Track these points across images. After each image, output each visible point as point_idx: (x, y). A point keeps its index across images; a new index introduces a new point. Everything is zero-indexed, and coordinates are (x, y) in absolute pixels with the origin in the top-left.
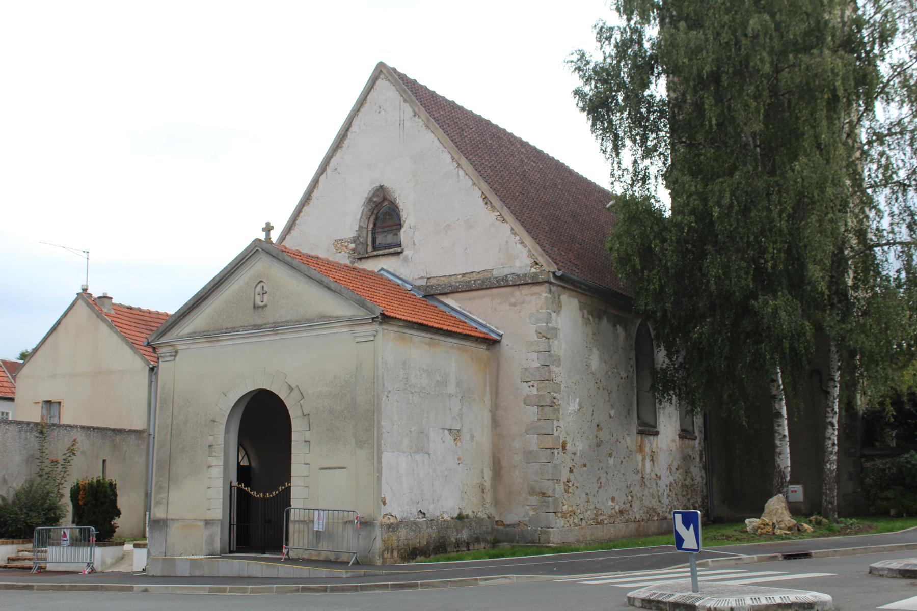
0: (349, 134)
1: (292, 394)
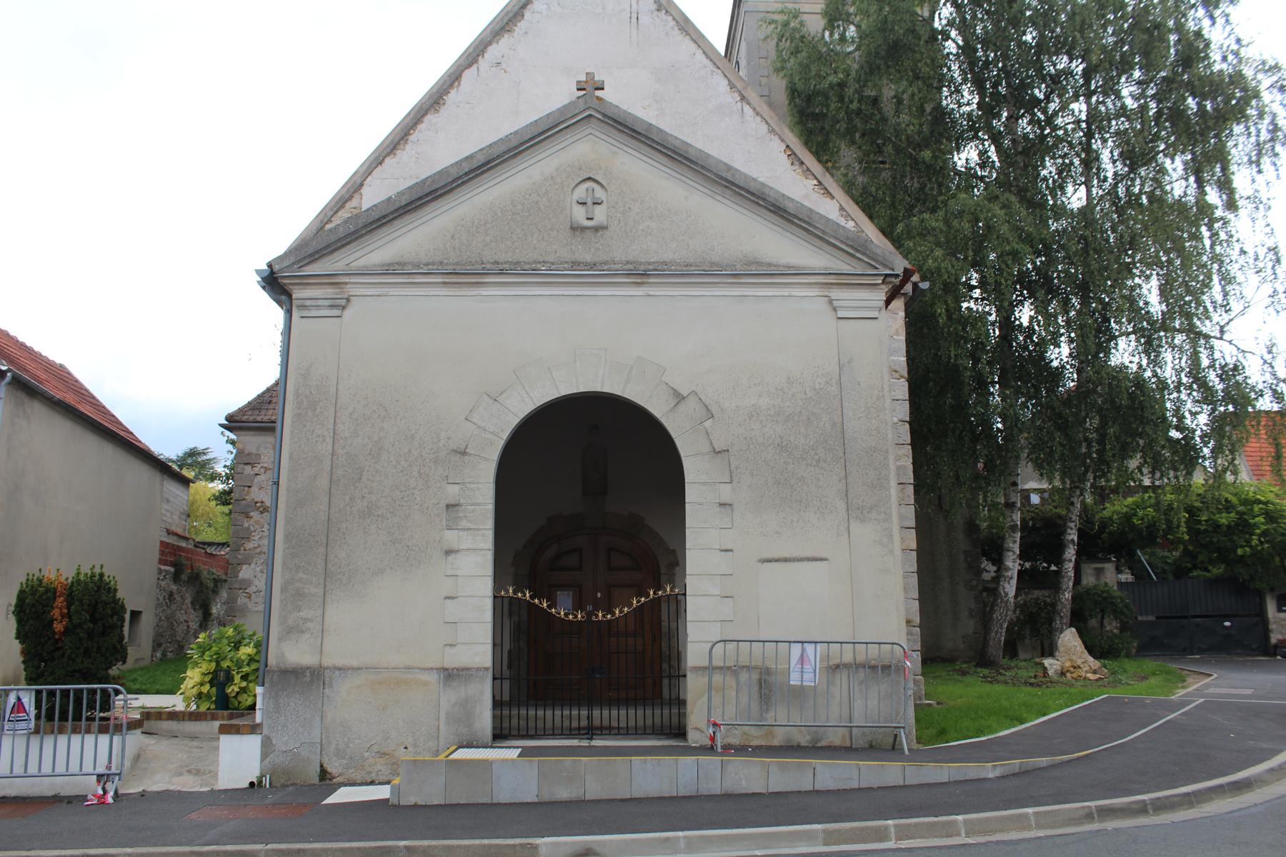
0: (527, 14)
1: (682, 407)
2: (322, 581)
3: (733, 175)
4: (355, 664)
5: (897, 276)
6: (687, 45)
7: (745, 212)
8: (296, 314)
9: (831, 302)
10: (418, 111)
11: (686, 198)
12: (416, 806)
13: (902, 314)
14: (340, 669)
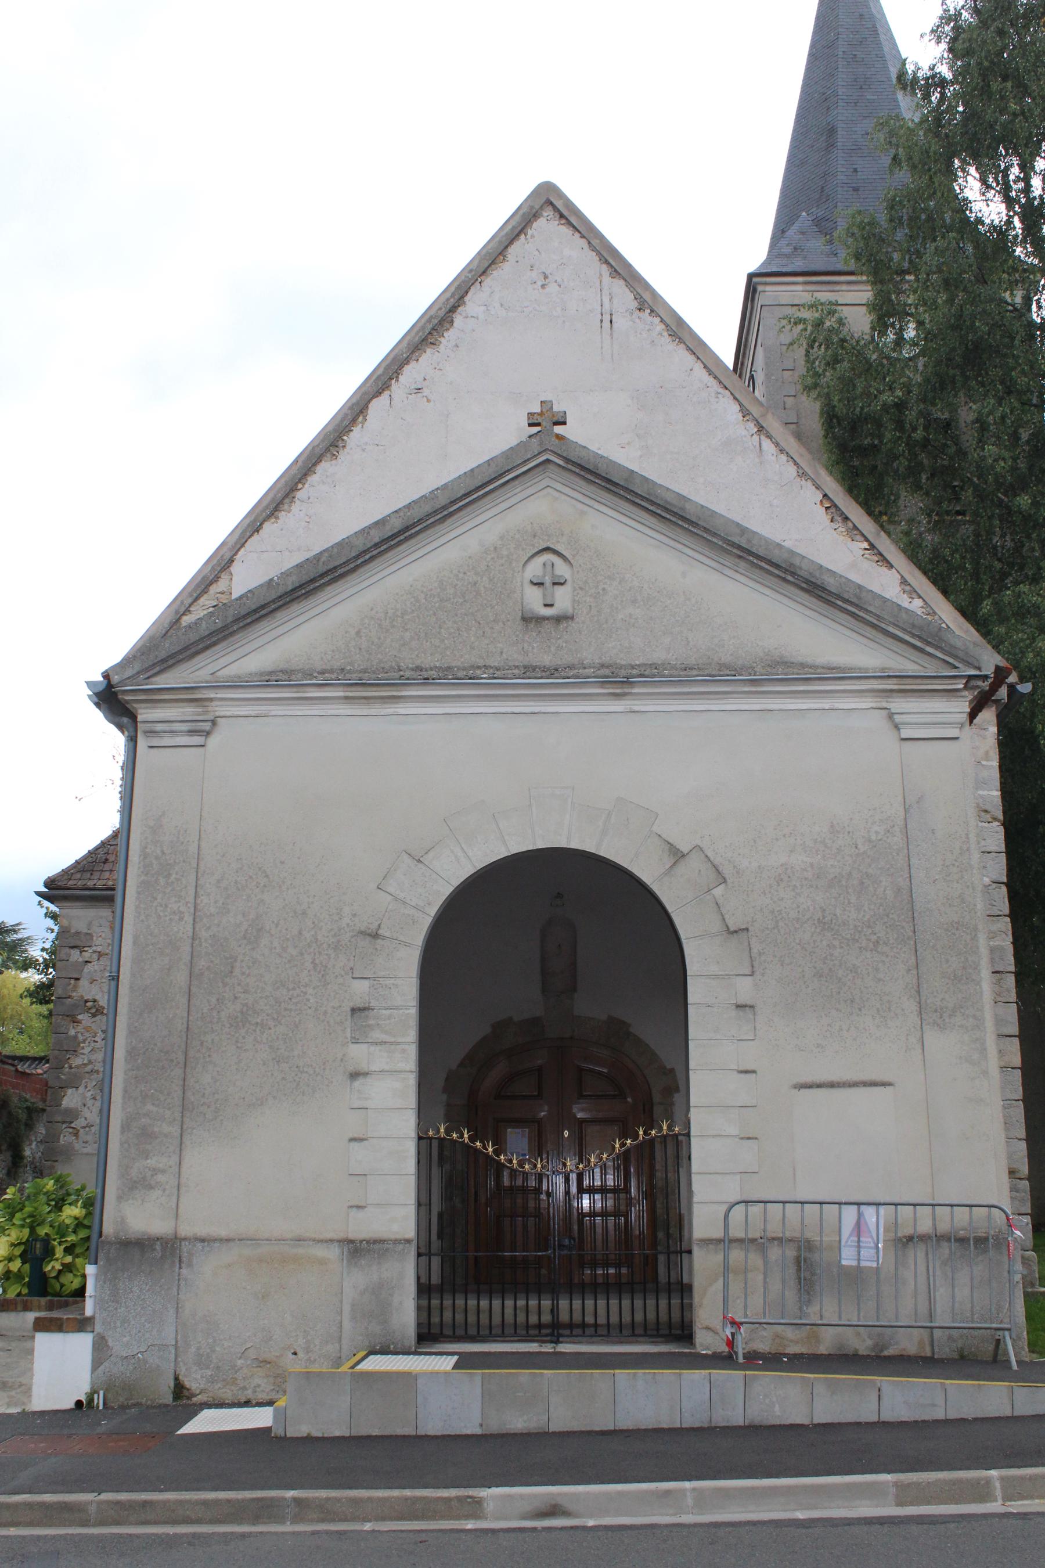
0: (458, 320)
2: (178, 1115)
3: (749, 541)
4: (223, 1233)
5: (985, 677)
6: (681, 355)
7: (768, 591)
8: (142, 742)
9: (891, 716)
10: (309, 458)
11: (684, 575)
12: (309, 1439)
13: (994, 729)
14: (203, 1240)
